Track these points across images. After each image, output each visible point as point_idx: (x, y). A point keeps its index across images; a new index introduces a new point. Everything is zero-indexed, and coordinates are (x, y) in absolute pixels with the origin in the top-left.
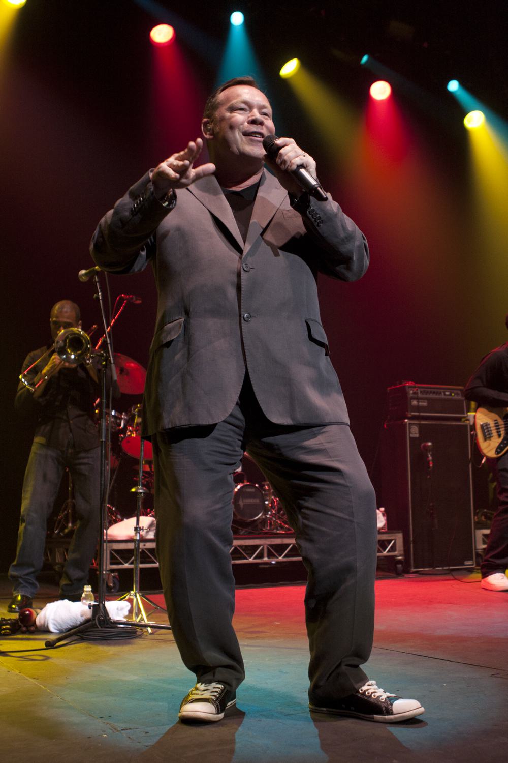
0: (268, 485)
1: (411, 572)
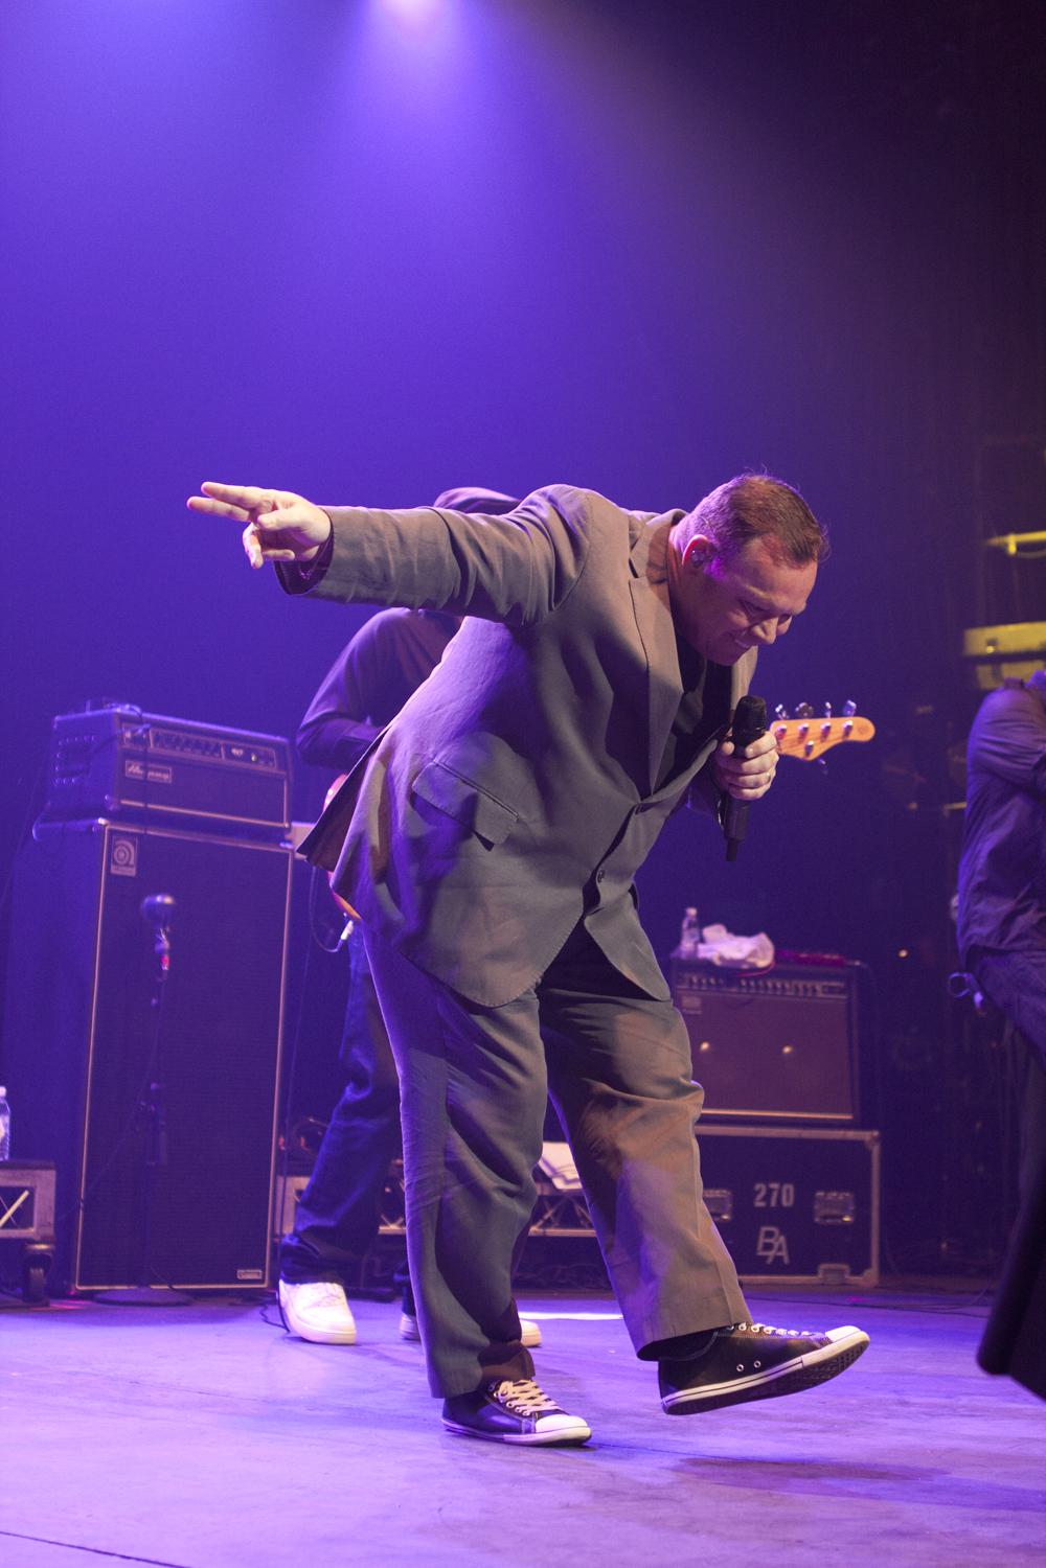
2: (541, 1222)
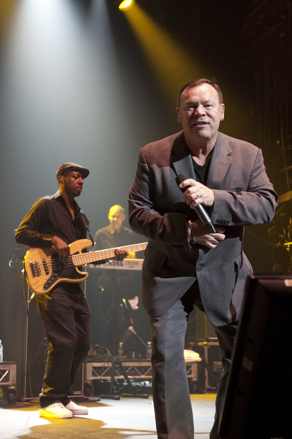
1: (24, 400)
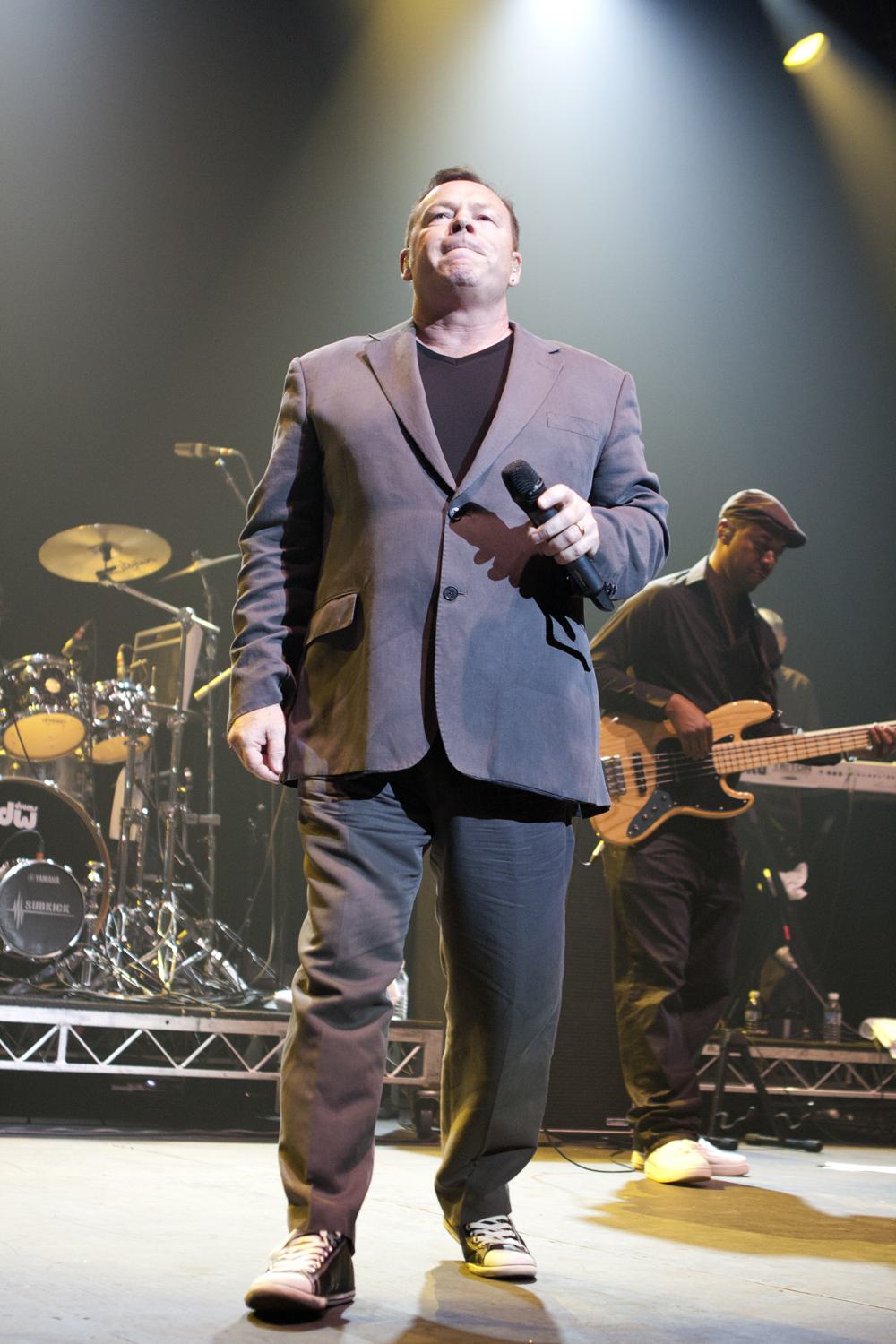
0: (100, 871)
2: (879, 1088)
